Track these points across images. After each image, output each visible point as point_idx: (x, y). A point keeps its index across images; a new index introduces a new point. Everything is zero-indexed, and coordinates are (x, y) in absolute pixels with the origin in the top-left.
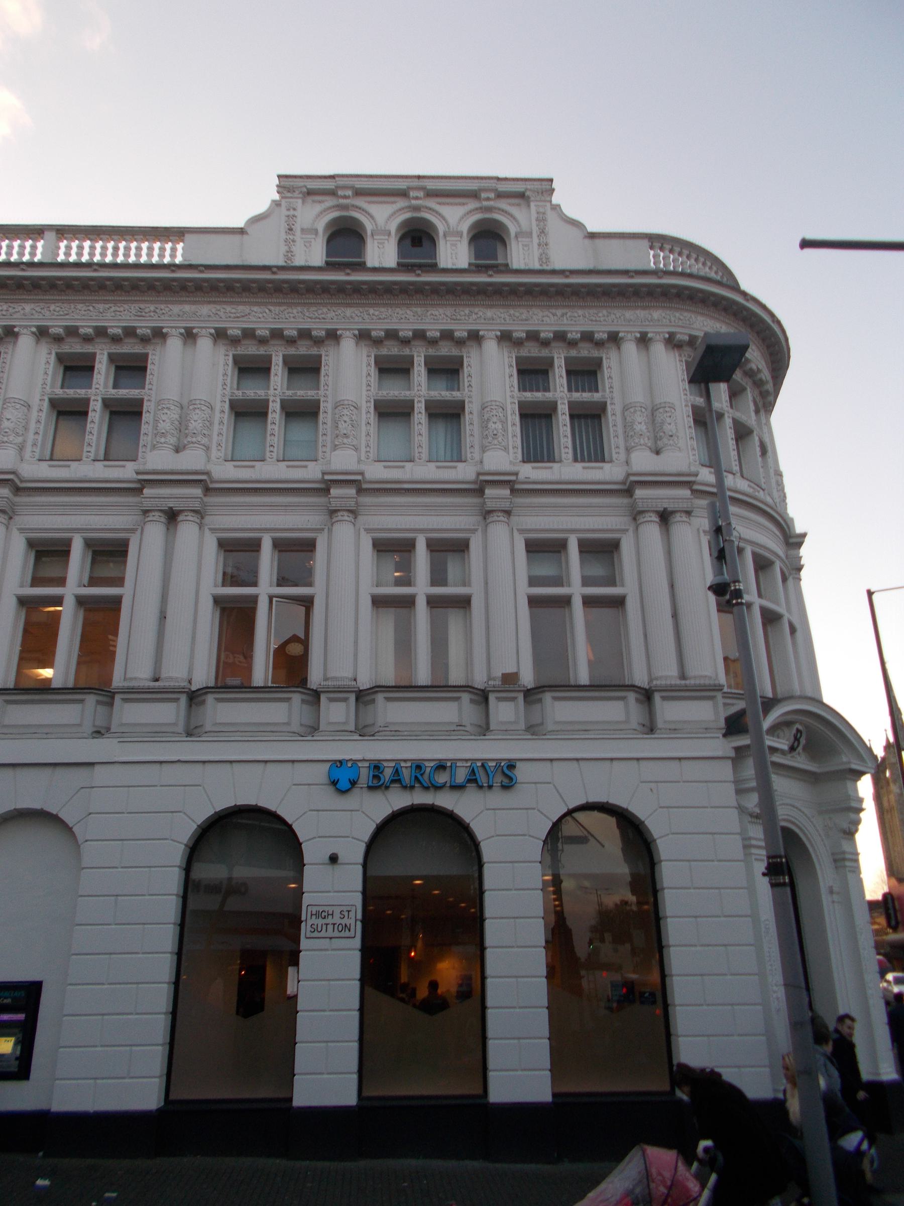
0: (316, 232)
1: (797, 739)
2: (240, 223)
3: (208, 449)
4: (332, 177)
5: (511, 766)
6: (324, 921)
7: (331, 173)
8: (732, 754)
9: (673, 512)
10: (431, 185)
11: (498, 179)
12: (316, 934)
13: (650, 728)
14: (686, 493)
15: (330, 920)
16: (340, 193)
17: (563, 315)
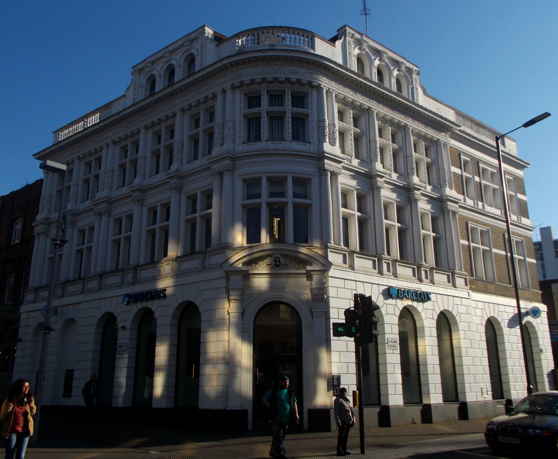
0: (142, 86)
1: (276, 261)
2: (123, 93)
3: (112, 186)
4: (144, 61)
5: (165, 290)
6: (122, 349)
7: (143, 60)
8: (224, 275)
9: (223, 171)
10: (170, 49)
11: (189, 34)
12: (119, 353)
13: (204, 268)
14: (227, 162)
15: (122, 349)
16: (148, 66)
17: (199, 92)
